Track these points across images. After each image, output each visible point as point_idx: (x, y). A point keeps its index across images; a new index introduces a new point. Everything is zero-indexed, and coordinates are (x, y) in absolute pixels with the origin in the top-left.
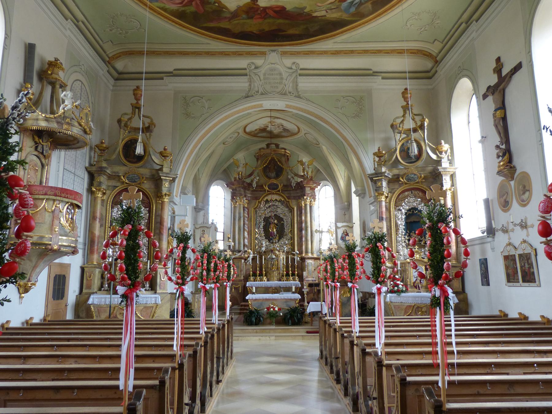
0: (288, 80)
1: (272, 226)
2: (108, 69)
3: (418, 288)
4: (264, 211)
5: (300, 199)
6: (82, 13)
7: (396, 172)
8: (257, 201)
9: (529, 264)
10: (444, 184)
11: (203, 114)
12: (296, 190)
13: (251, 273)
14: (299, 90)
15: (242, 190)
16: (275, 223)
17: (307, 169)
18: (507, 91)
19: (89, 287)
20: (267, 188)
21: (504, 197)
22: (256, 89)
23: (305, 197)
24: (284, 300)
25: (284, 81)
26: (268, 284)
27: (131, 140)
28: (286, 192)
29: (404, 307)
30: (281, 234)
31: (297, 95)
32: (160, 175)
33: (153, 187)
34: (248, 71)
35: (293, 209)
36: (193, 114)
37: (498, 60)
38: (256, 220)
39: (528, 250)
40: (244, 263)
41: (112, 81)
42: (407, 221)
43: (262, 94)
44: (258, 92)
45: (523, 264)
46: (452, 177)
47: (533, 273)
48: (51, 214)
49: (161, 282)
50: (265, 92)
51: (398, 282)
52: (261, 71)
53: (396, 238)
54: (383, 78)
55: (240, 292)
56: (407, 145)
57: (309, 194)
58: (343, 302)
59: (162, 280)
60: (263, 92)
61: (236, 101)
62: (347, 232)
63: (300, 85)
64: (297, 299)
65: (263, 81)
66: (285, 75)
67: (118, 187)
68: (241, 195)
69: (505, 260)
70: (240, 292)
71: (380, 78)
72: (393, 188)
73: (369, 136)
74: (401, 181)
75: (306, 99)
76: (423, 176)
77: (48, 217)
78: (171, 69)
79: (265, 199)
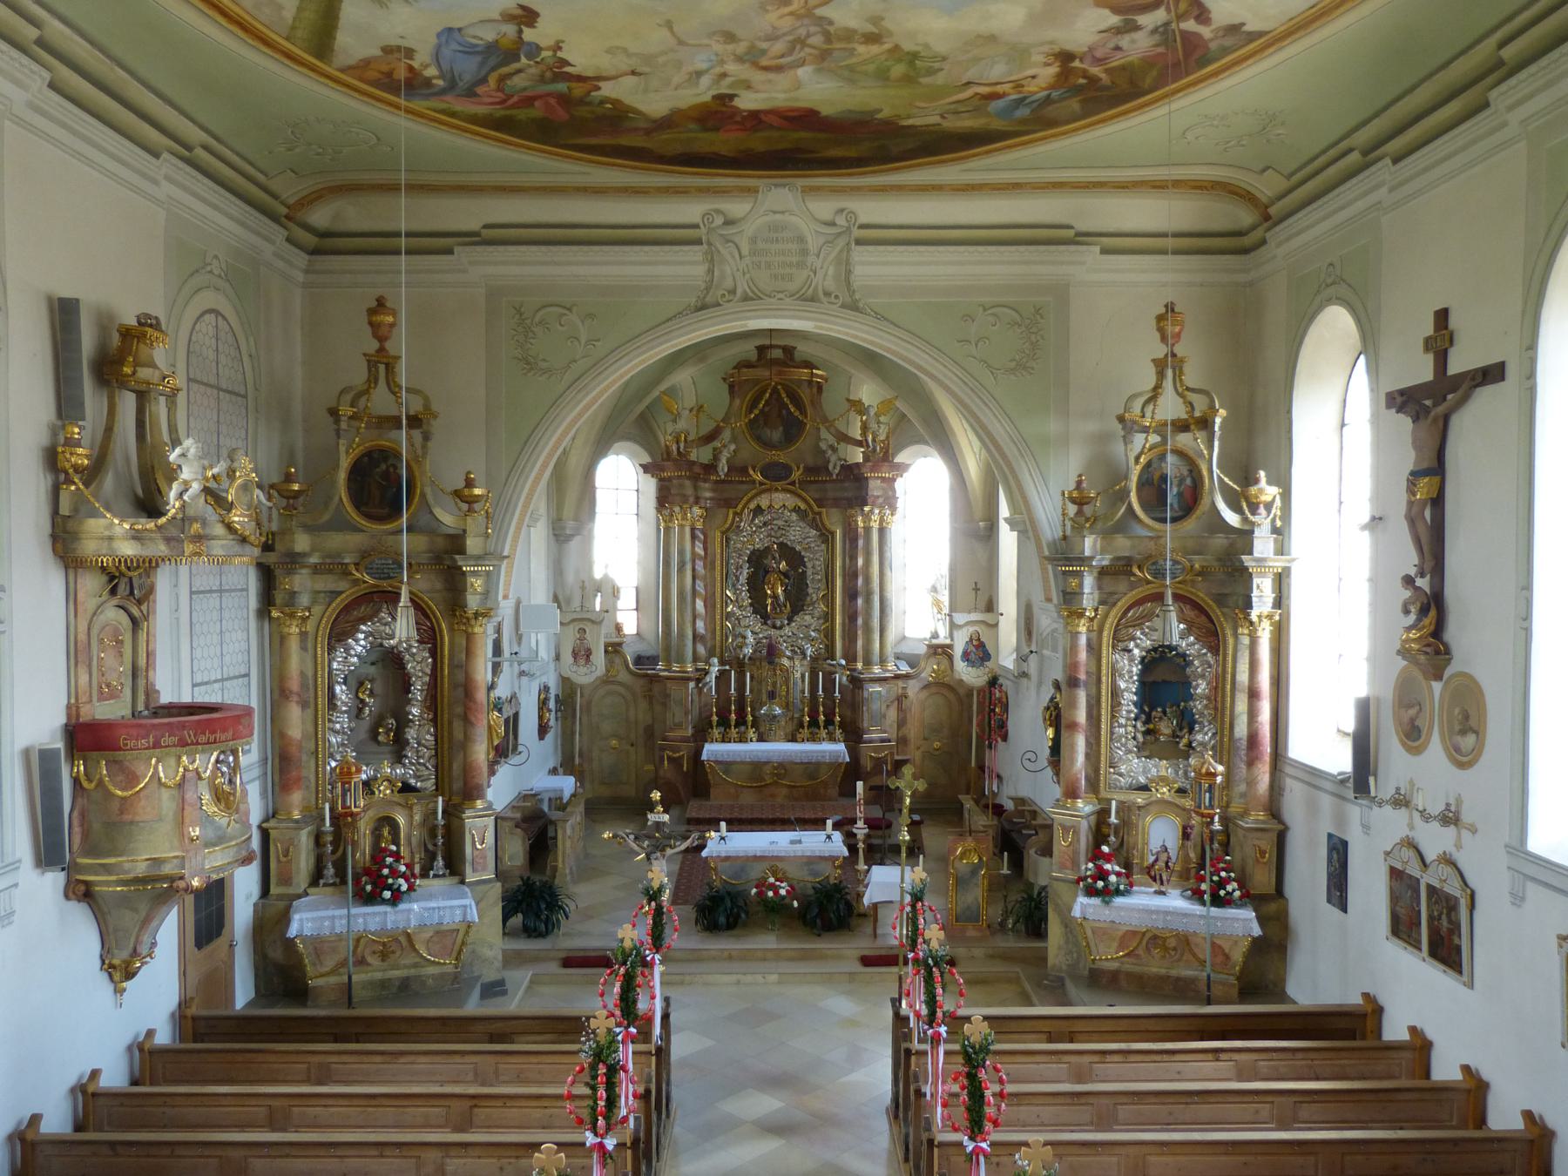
0: (821, 255)
1: (773, 577)
2: (286, 233)
3: (1158, 881)
4: (752, 537)
5: (851, 506)
6: (202, 127)
7: (1123, 545)
8: (731, 511)
9: (1450, 921)
10: (1254, 599)
11: (575, 361)
12: (842, 481)
13: (715, 718)
14: (856, 284)
15: (688, 483)
17: (874, 426)
18: (1455, 421)
19: (286, 880)
20: (758, 477)
21: (1412, 712)
22: (729, 283)
23: (867, 509)
24: (805, 860)
25: (811, 259)
27: (369, 454)
28: (814, 486)
29: (1120, 933)
30: (797, 601)
31: (848, 300)
32: (460, 563)
33: (439, 586)
34: (703, 230)
35: (833, 534)
36: (544, 360)
37: (1442, 317)
38: (727, 564)
39: (1453, 888)
40: (695, 691)
41: (302, 259)
42: (1146, 680)
43: (746, 298)
44: (733, 292)
45: (1436, 913)
46: (1281, 581)
47: (1458, 949)
48: (175, 792)
49: (476, 853)
50: (755, 294)
51: (1108, 867)
52: (743, 231)
53: (1112, 727)
54: (1105, 251)
55: (685, 769)
56: (1161, 468)
57: (878, 497)
58: (960, 875)
59: (479, 847)
60: (751, 294)
61: (670, 319)
62: (979, 639)
63: (858, 271)
64: (837, 858)
65: (747, 260)
66: (812, 243)
67: (341, 593)
68: (685, 499)
69: (1391, 877)
70: (685, 769)
71: (1097, 249)
72: (1112, 589)
73: (1053, 426)
74: (1134, 575)
75: (876, 313)
76: (1197, 566)
77: (167, 802)
78: (473, 225)
79: (752, 506)
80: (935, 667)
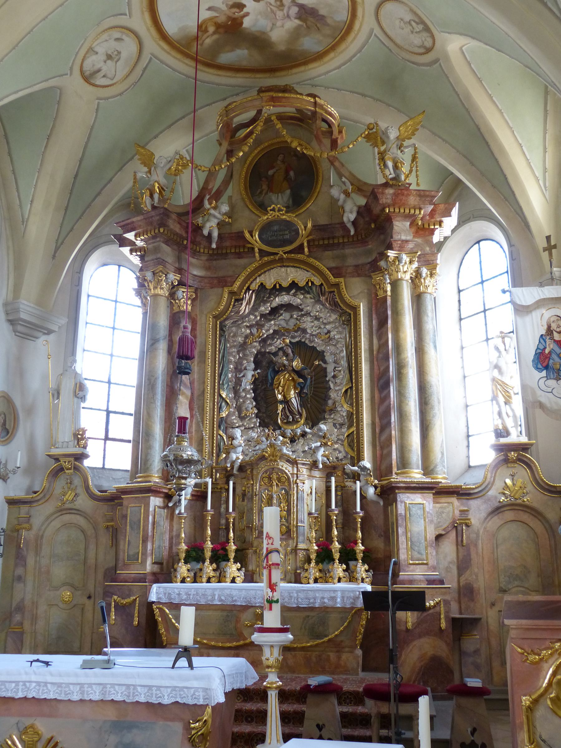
1: (283, 378)
8: (226, 290)
12: (364, 242)
16: (293, 370)
17: (394, 151)
24: (111, 714)
26: (234, 593)
28: (329, 253)
35: (355, 309)
57: (407, 241)
70: (136, 623)
79: (255, 286)
80: (509, 482)
